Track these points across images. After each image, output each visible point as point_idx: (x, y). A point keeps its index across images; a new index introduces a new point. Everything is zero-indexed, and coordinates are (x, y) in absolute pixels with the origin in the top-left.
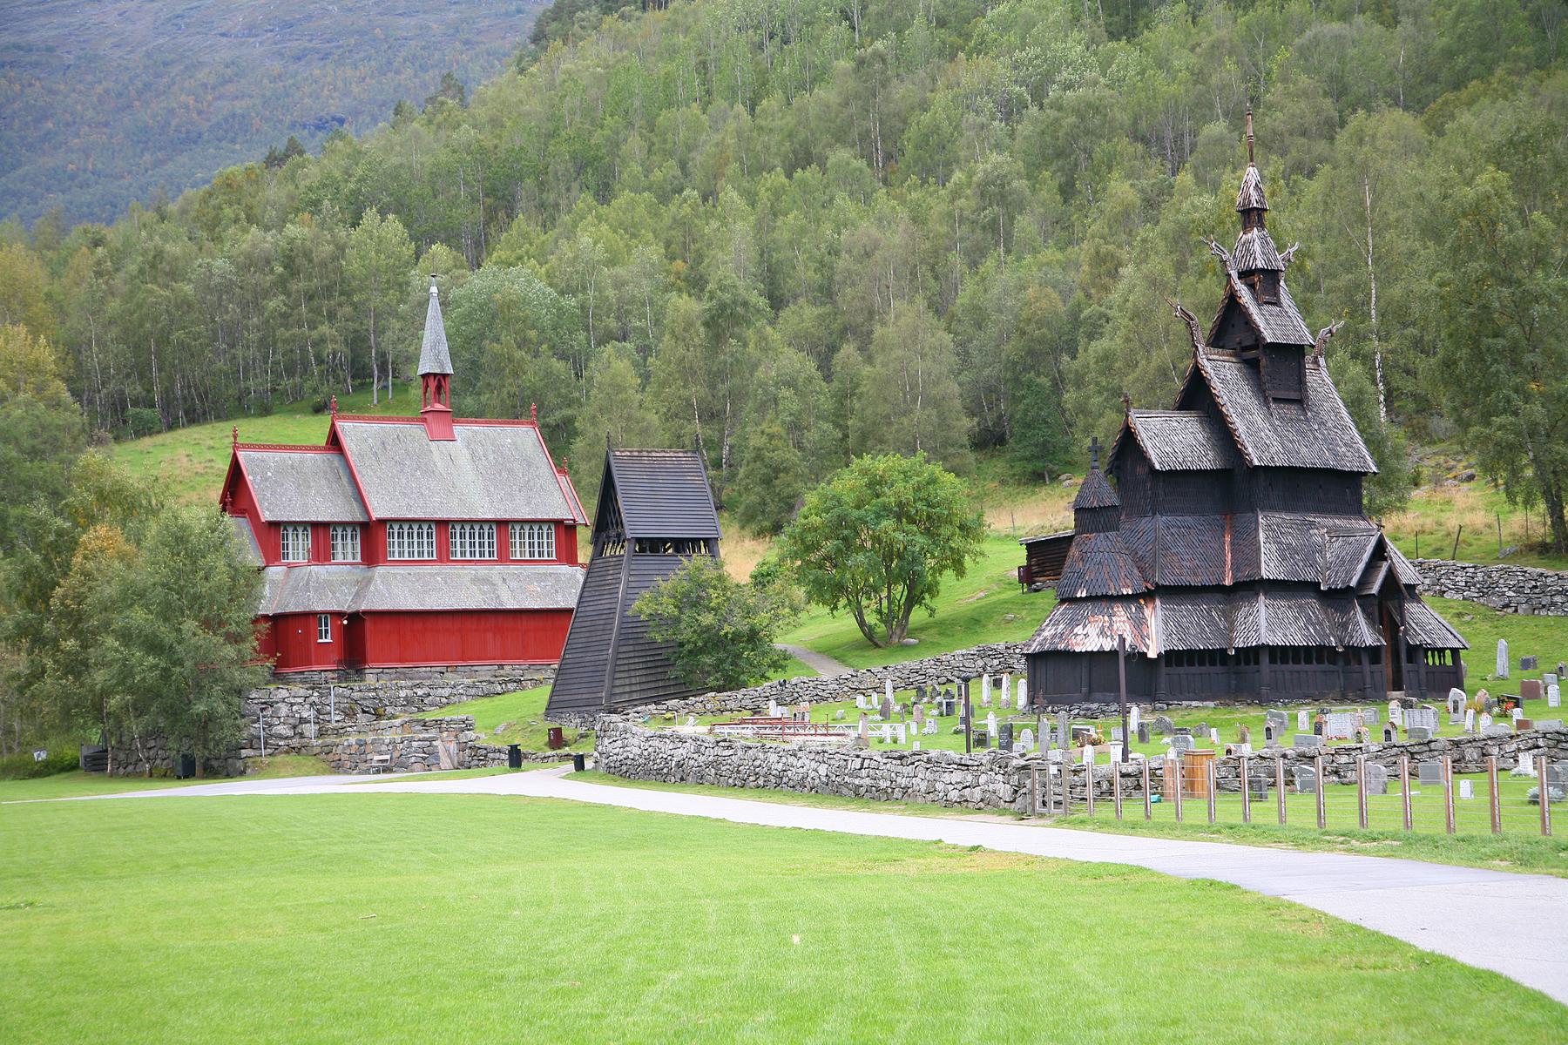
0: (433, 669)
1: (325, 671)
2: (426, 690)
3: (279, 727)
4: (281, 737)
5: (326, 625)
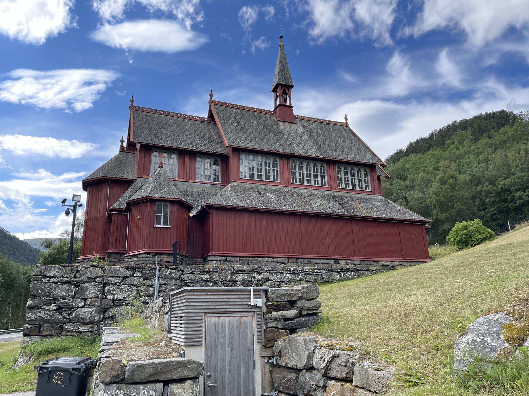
0: (275, 260)
2: (266, 275)
3: (83, 310)
4: (82, 322)
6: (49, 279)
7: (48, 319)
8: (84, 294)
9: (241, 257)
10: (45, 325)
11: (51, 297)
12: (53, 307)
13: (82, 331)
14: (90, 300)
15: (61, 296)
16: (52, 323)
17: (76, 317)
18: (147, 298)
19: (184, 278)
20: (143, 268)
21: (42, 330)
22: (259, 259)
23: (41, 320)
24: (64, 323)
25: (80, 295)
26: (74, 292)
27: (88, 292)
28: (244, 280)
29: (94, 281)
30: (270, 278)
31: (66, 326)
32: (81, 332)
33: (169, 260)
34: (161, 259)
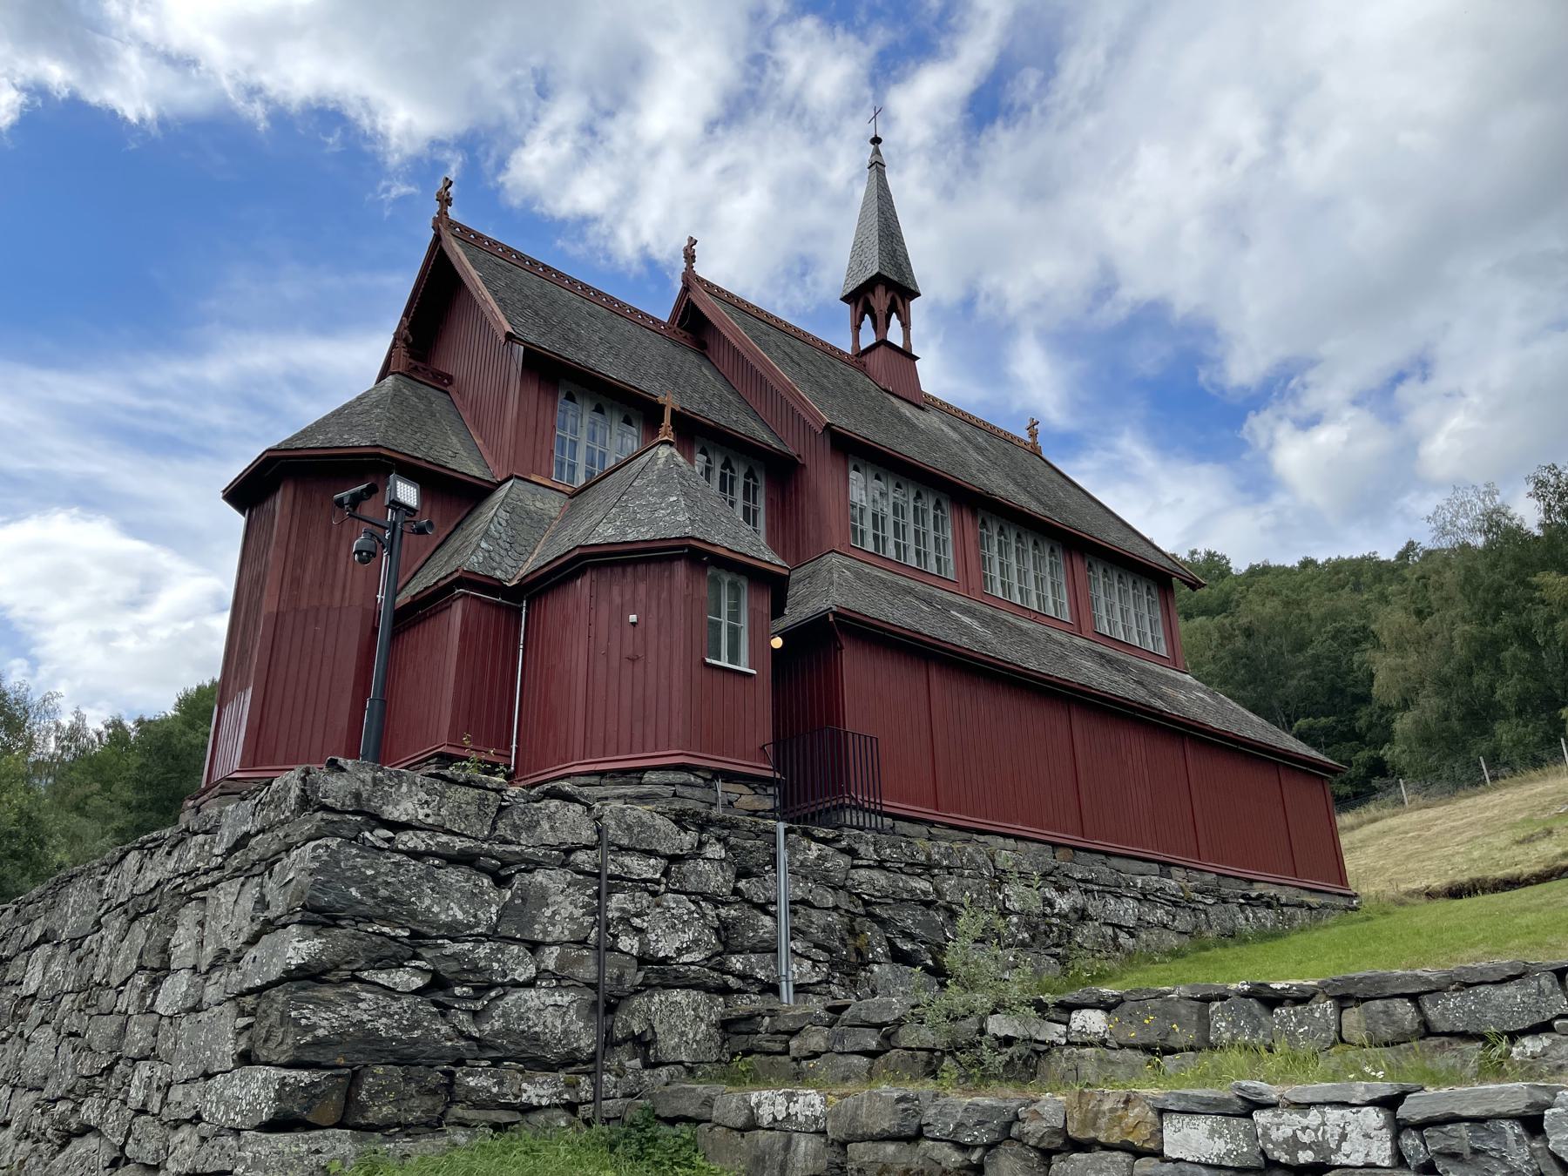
1: (730, 777)
5: (734, 616)
6: (391, 834)
7: (393, 1039)
8: (533, 920)
9: (932, 824)
10: (380, 1070)
11: (403, 927)
12: (407, 979)
13: (535, 1101)
14: (556, 950)
15: (445, 924)
17: (507, 1032)
18: (753, 958)
19: (860, 884)
20: (733, 826)
21: (363, 1095)
22: (982, 838)
23: (360, 1041)
24: (460, 1062)
26: (494, 909)
27: (548, 913)
29: (563, 865)
30: (1090, 910)
31: (468, 1075)
32: (528, 1109)
33: (757, 805)
34: (733, 797)
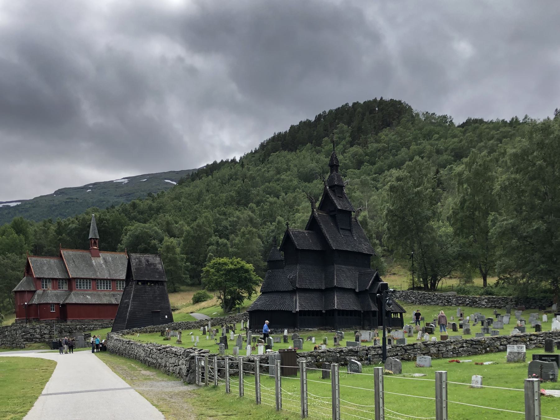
2: (86, 326)
16: (30, 338)
25: (35, 332)
28: (79, 327)
